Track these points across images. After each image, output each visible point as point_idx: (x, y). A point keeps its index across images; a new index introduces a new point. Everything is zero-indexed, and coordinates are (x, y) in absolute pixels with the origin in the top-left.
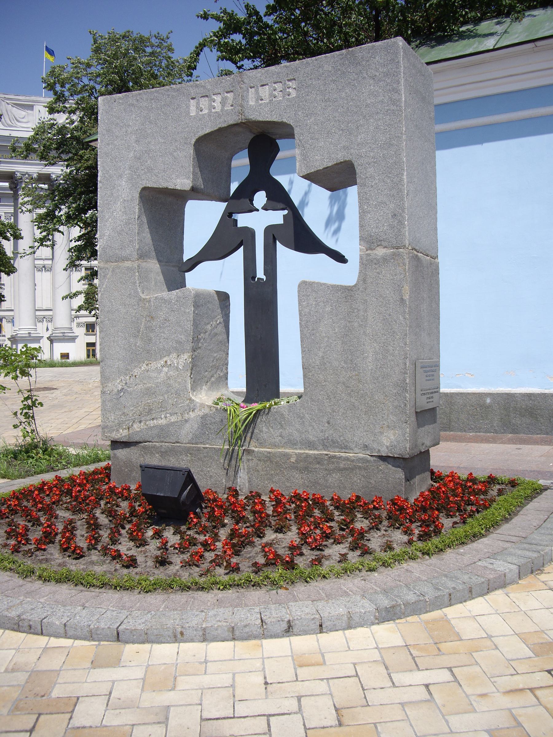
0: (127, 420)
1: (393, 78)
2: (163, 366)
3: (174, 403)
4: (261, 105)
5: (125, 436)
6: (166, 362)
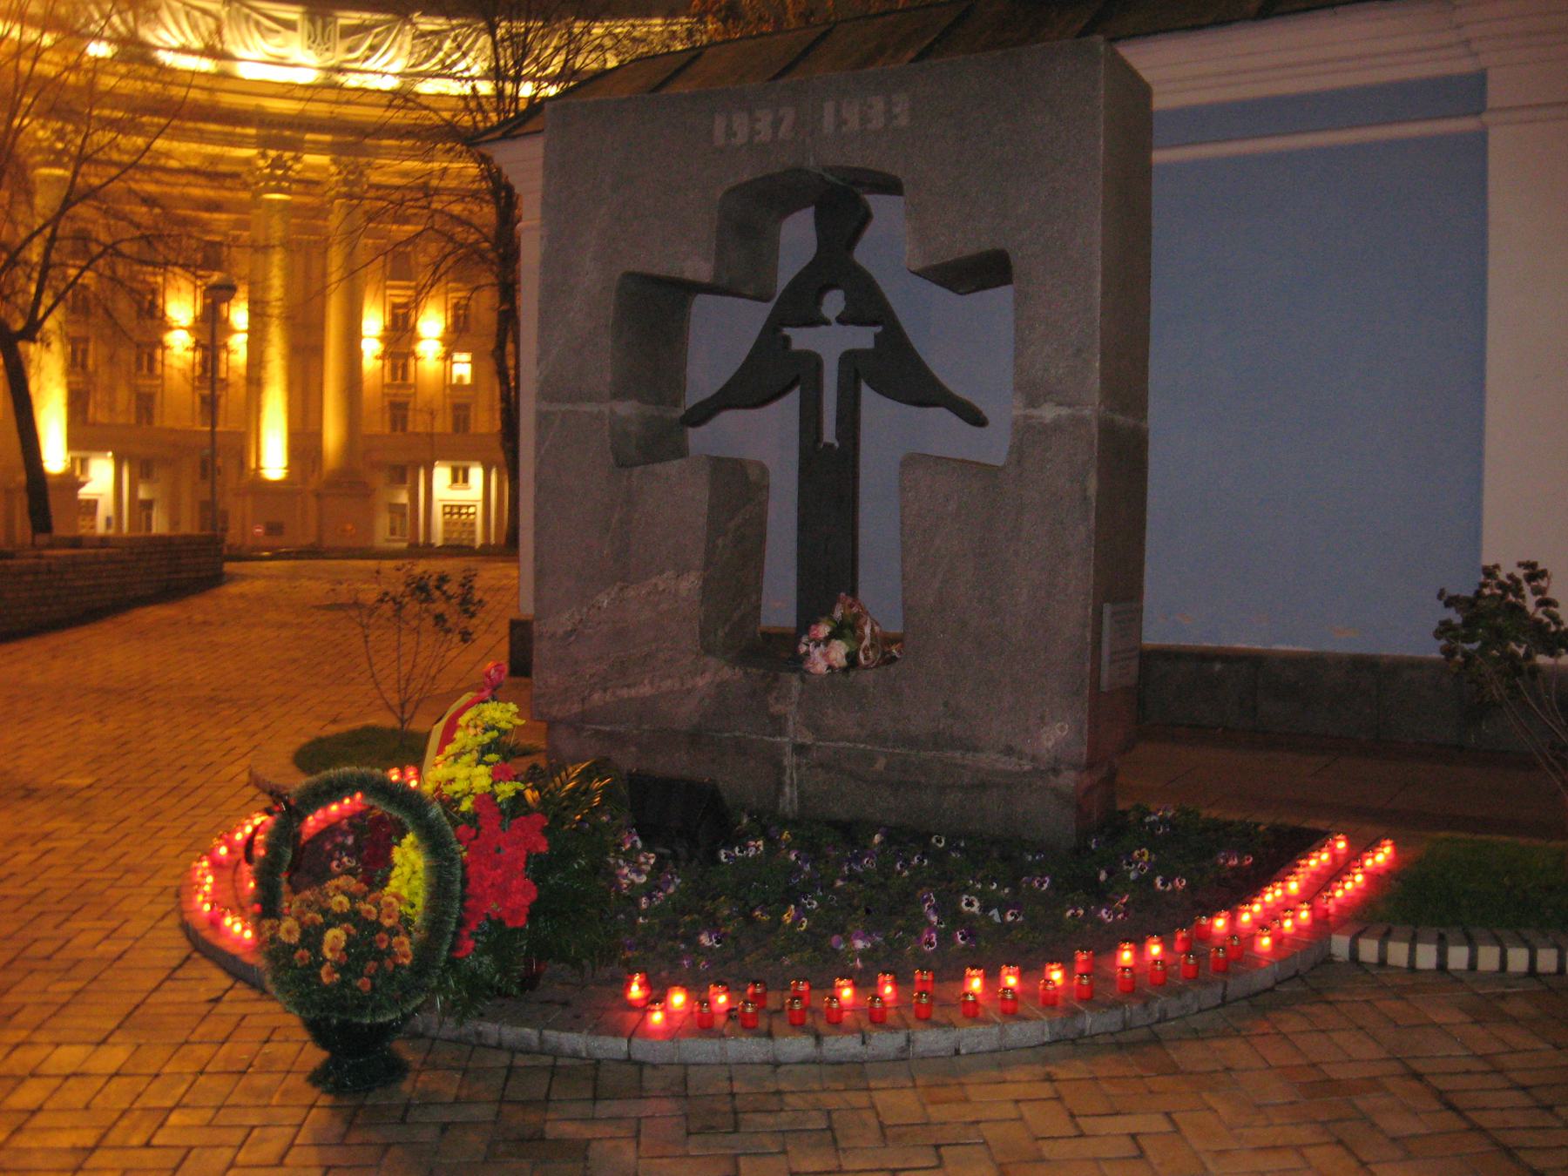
6: (656, 585)
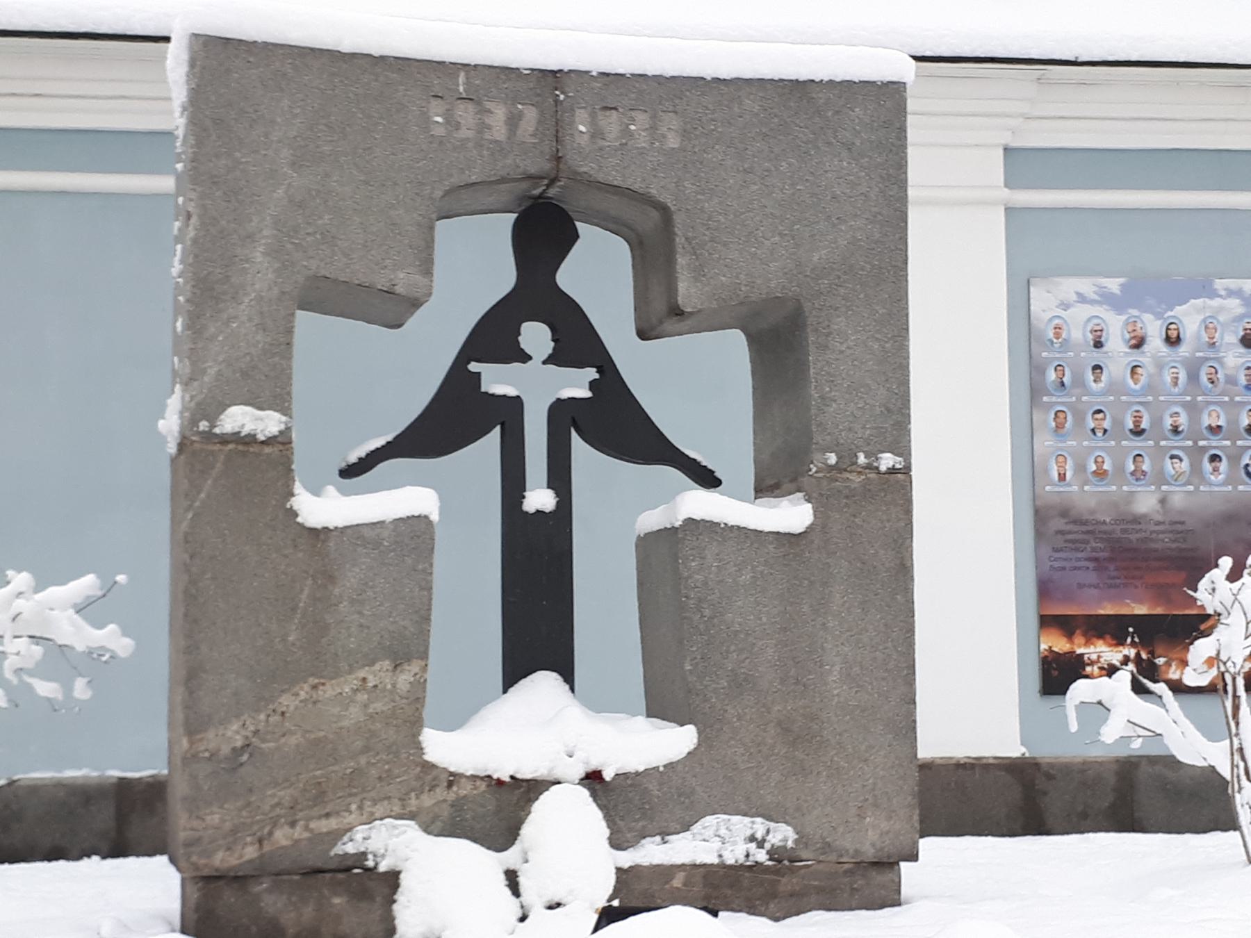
0: (258, 822)
1: (890, 156)
2: (355, 691)
3: (384, 775)
4: (601, 149)
5: (250, 861)
6: (364, 679)
